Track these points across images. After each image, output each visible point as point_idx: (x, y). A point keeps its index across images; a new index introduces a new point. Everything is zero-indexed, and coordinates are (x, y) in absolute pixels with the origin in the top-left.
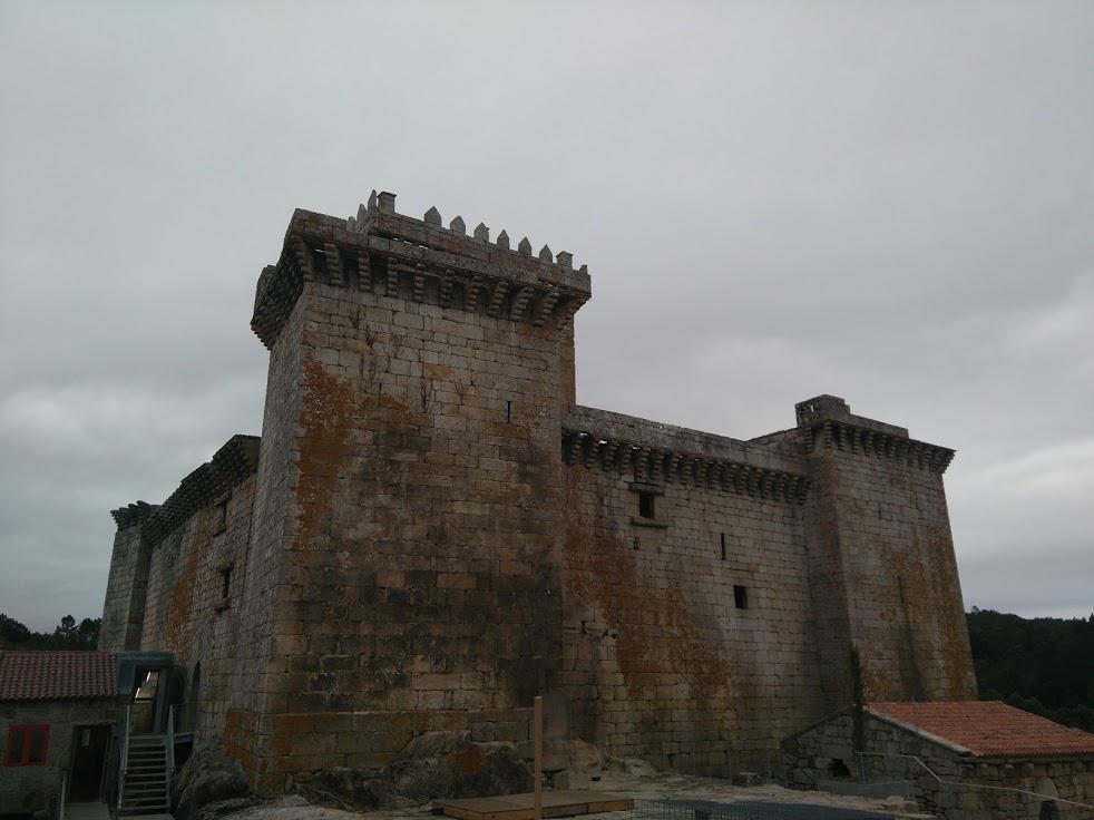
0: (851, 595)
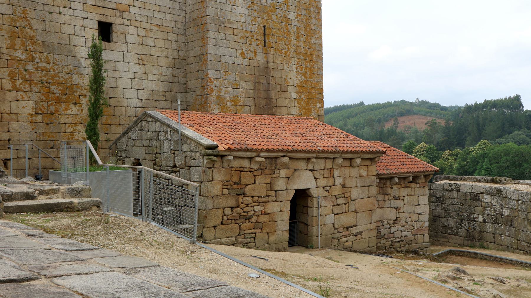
0: (212, 35)
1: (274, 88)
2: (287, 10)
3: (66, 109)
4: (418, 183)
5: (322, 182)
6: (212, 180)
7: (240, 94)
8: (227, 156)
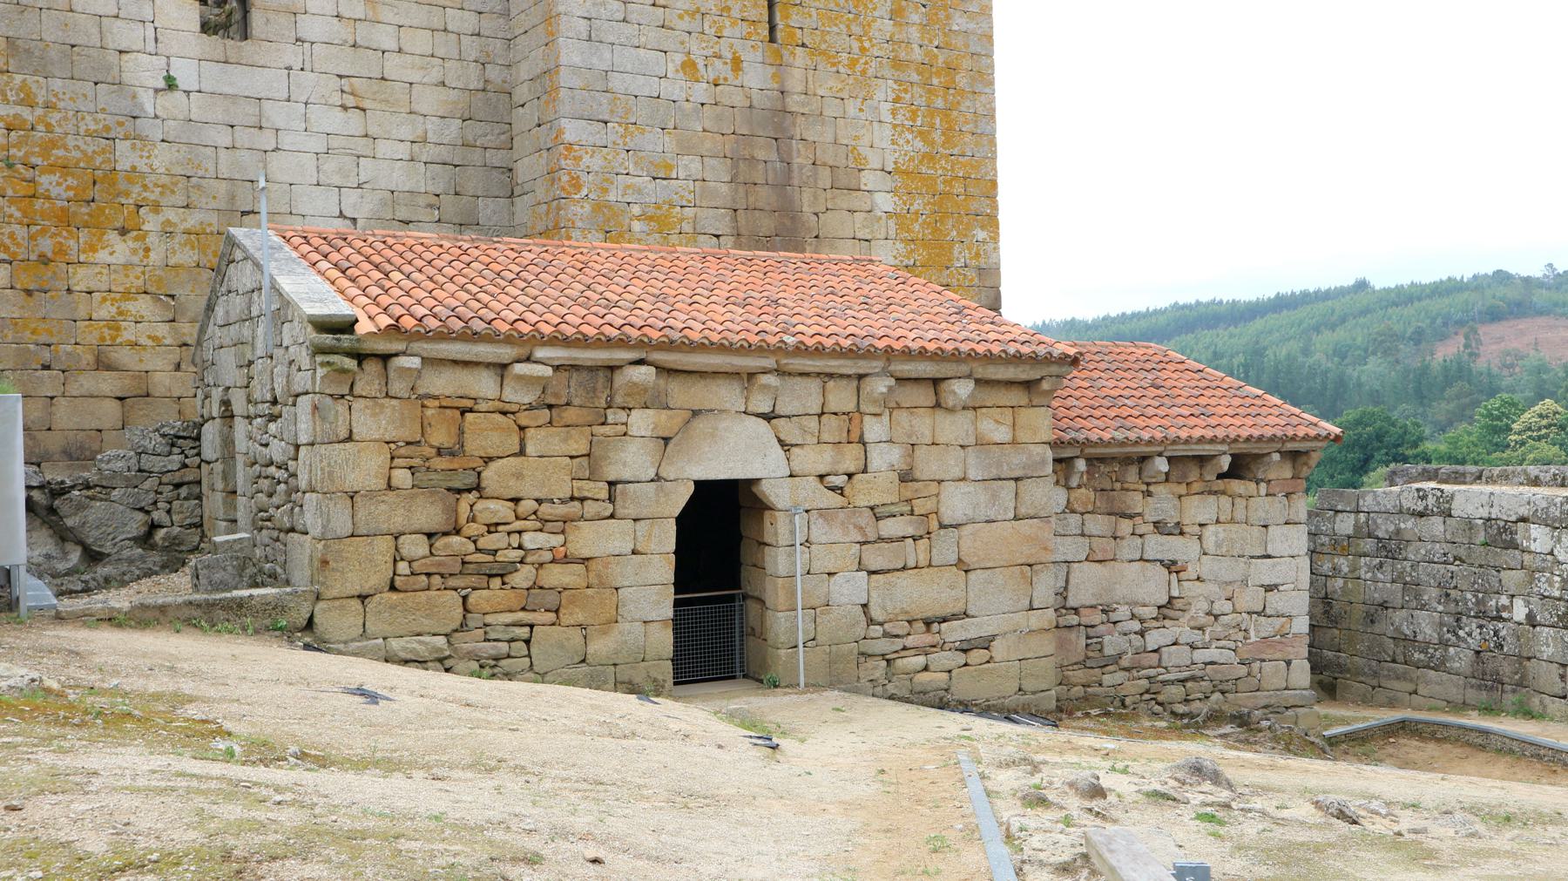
1: (808, 177)
3: (93, 249)
4: (1262, 480)
5: (813, 459)
6: (350, 439)
7: (682, 197)
8: (396, 355)
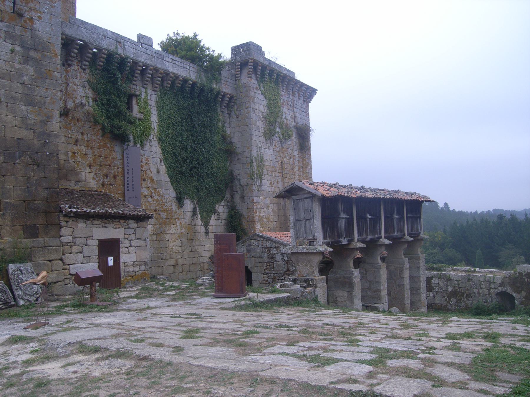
2: (293, 150)
